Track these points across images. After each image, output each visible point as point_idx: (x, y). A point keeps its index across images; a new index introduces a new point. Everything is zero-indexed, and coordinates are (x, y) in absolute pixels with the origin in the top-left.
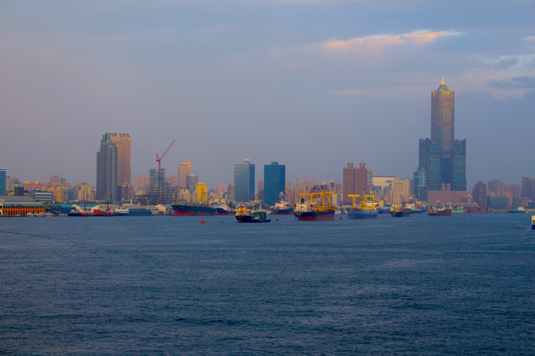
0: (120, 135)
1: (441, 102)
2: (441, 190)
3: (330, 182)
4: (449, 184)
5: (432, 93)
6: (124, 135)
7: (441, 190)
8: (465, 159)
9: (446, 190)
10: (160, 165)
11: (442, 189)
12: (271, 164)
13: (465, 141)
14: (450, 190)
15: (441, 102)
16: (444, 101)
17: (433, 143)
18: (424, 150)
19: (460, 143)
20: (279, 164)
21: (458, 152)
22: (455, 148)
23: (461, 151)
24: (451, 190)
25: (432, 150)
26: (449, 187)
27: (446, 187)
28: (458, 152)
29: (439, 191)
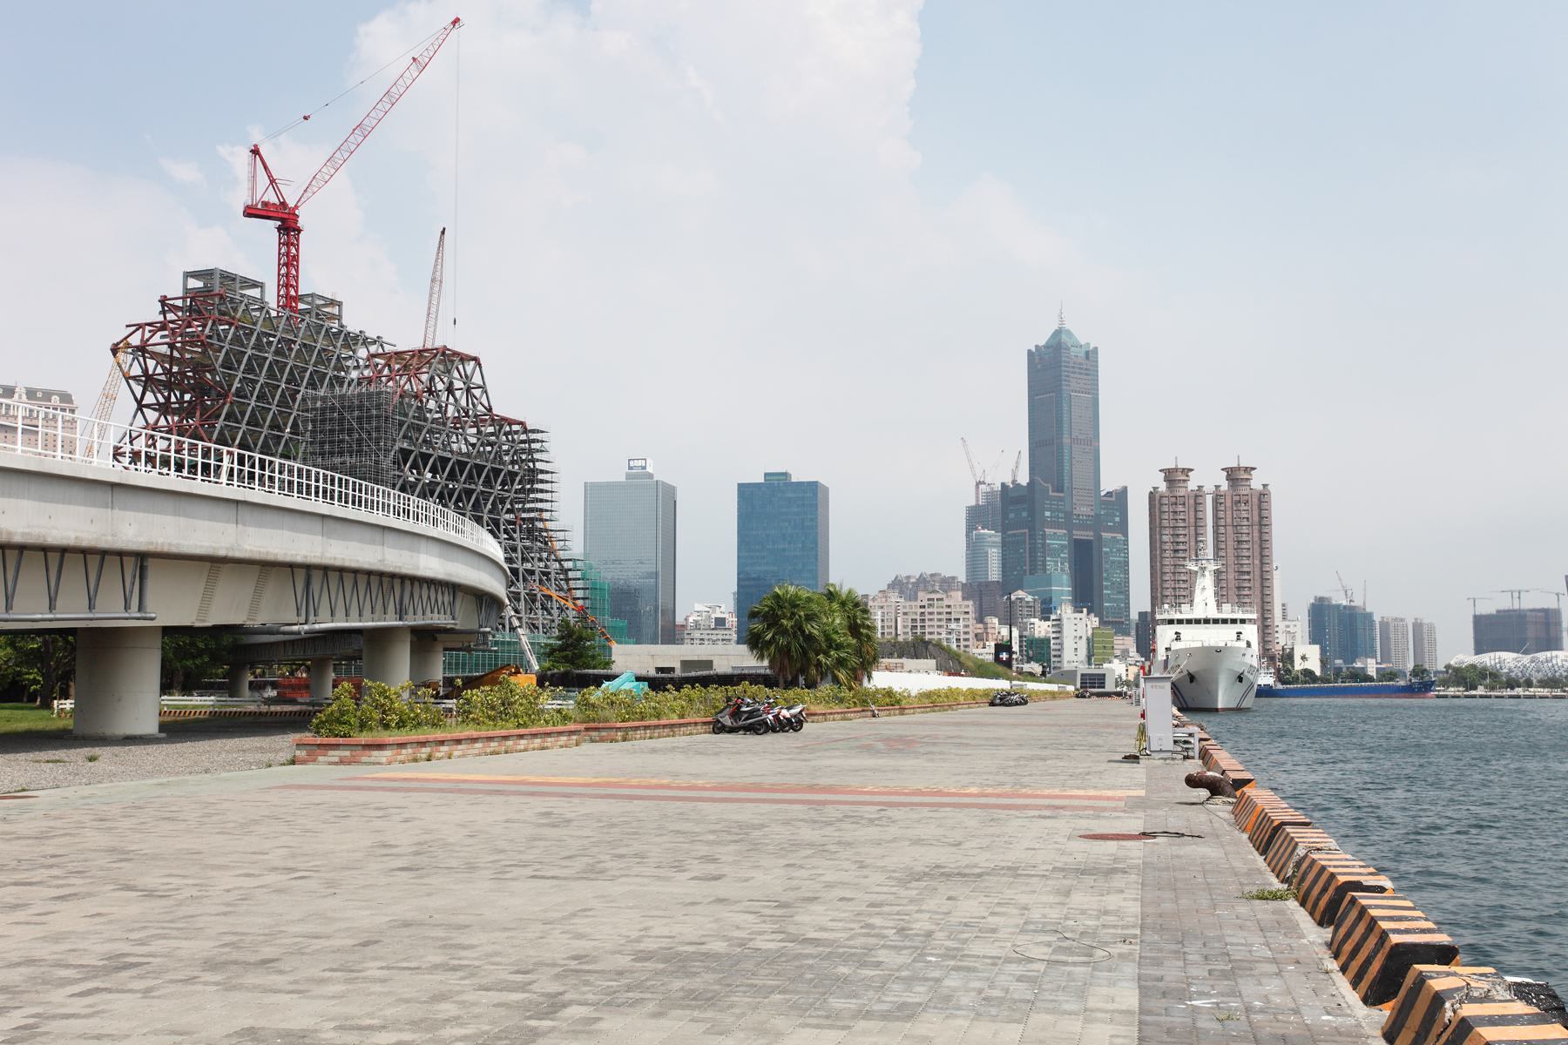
0: (31, 394)
3: (713, 616)
5: (1029, 351)
6: (47, 395)
8: (1126, 542)
10: (289, 262)
12: (763, 481)
13: (1125, 490)
15: (1068, 376)
16: (1075, 373)
17: (1051, 494)
18: (1024, 514)
19: (1113, 499)
20: (794, 479)
23: (1117, 519)
25: (1047, 514)
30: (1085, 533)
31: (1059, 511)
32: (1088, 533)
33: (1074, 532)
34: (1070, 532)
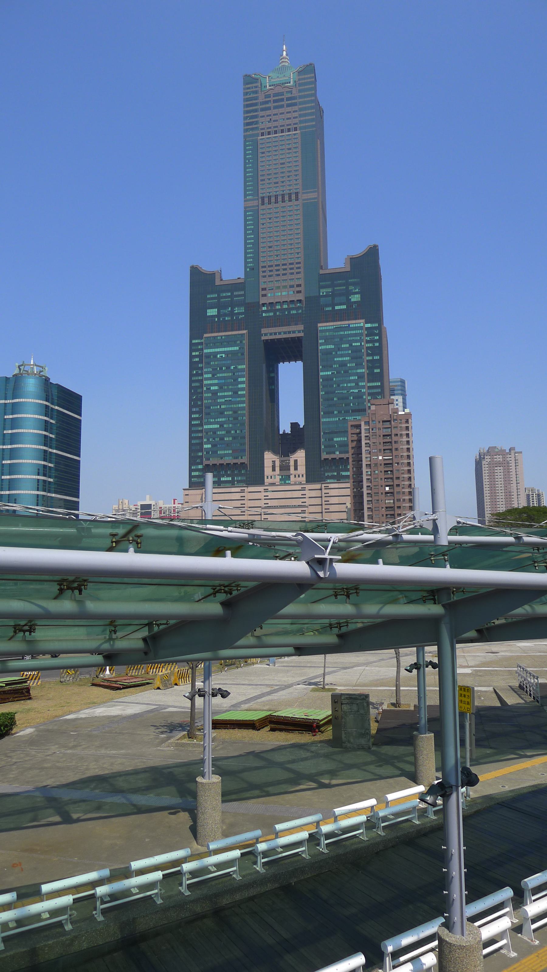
1: (256, 116)
2: (261, 482)
4: (300, 456)
7: (261, 482)
9: (285, 479)
11: (267, 481)
13: (373, 252)
14: (304, 479)
15: (256, 116)
21: (337, 308)
22: (323, 292)
23: (356, 298)
24: (308, 481)
25: (212, 312)
26: (302, 469)
27: (285, 468)
28: (337, 308)
29: (251, 489)
30: (286, 329)
31: (233, 305)
32: (293, 328)
33: (264, 331)
34: (254, 335)
